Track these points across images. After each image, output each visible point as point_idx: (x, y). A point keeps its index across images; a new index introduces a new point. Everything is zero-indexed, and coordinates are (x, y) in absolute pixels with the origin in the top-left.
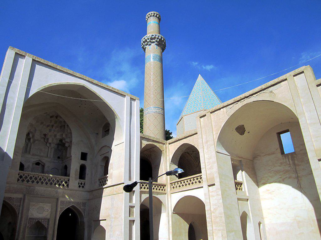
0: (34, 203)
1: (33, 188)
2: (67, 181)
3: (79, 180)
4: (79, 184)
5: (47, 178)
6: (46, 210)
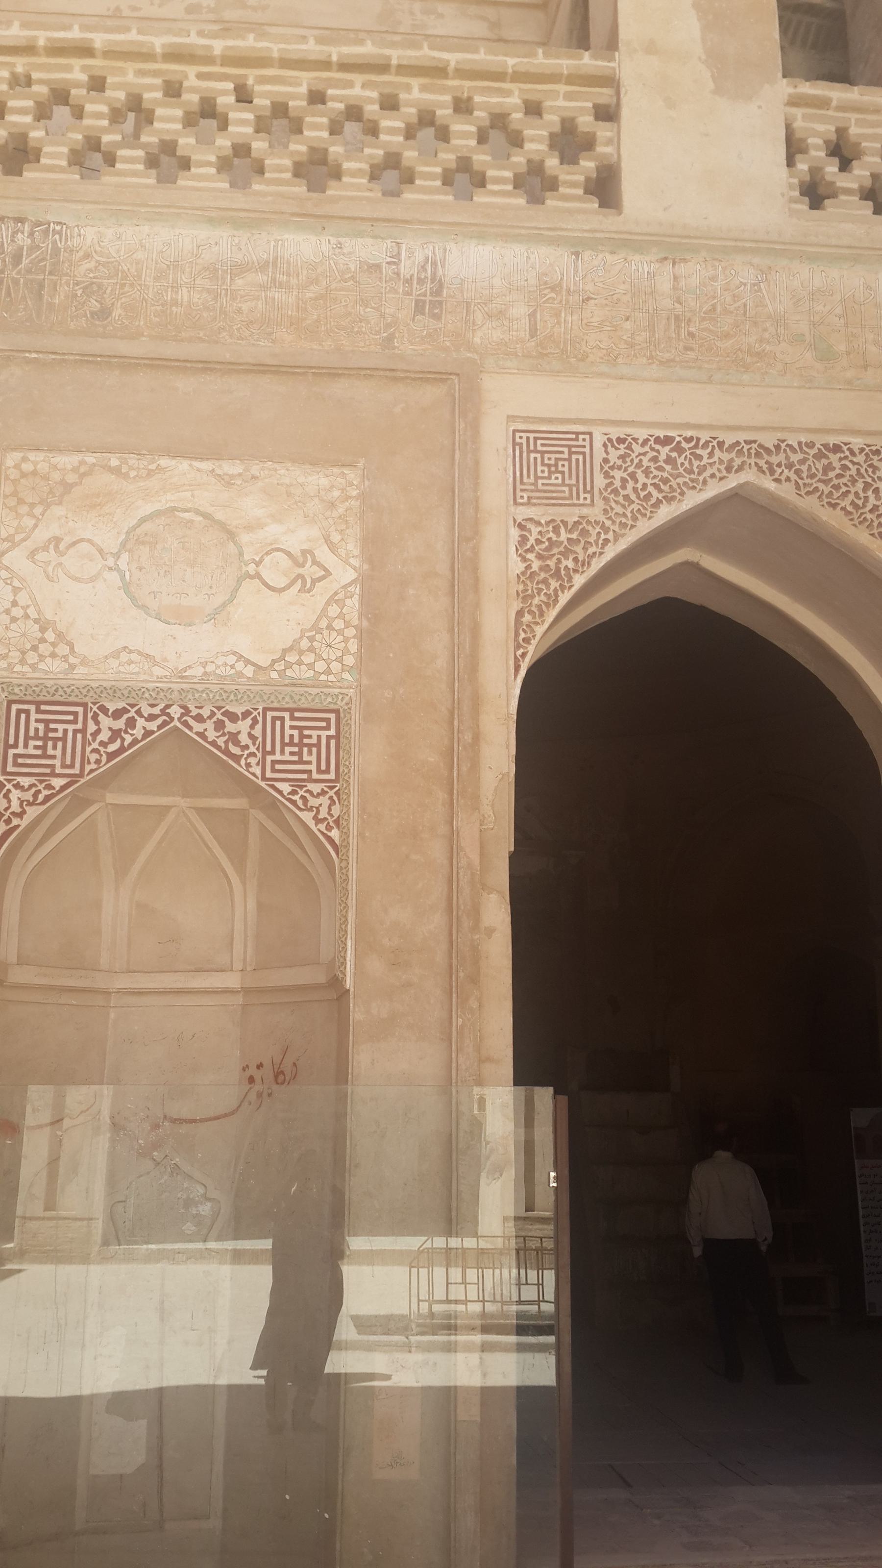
0: (67, 461)
1: (23, 239)
2: (586, 122)
3: (784, 88)
4: (794, 147)
5: (243, 96)
6: (275, 570)
